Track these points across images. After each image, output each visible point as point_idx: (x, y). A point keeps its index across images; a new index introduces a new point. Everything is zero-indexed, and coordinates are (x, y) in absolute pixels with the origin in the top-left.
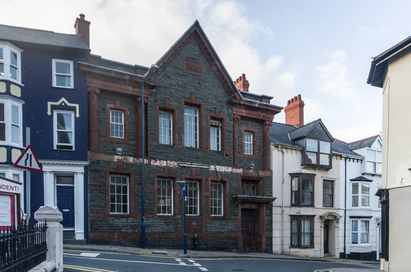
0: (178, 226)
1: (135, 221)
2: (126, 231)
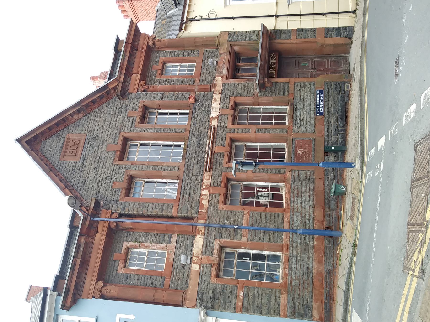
0: (303, 176)
1: (294, 245)
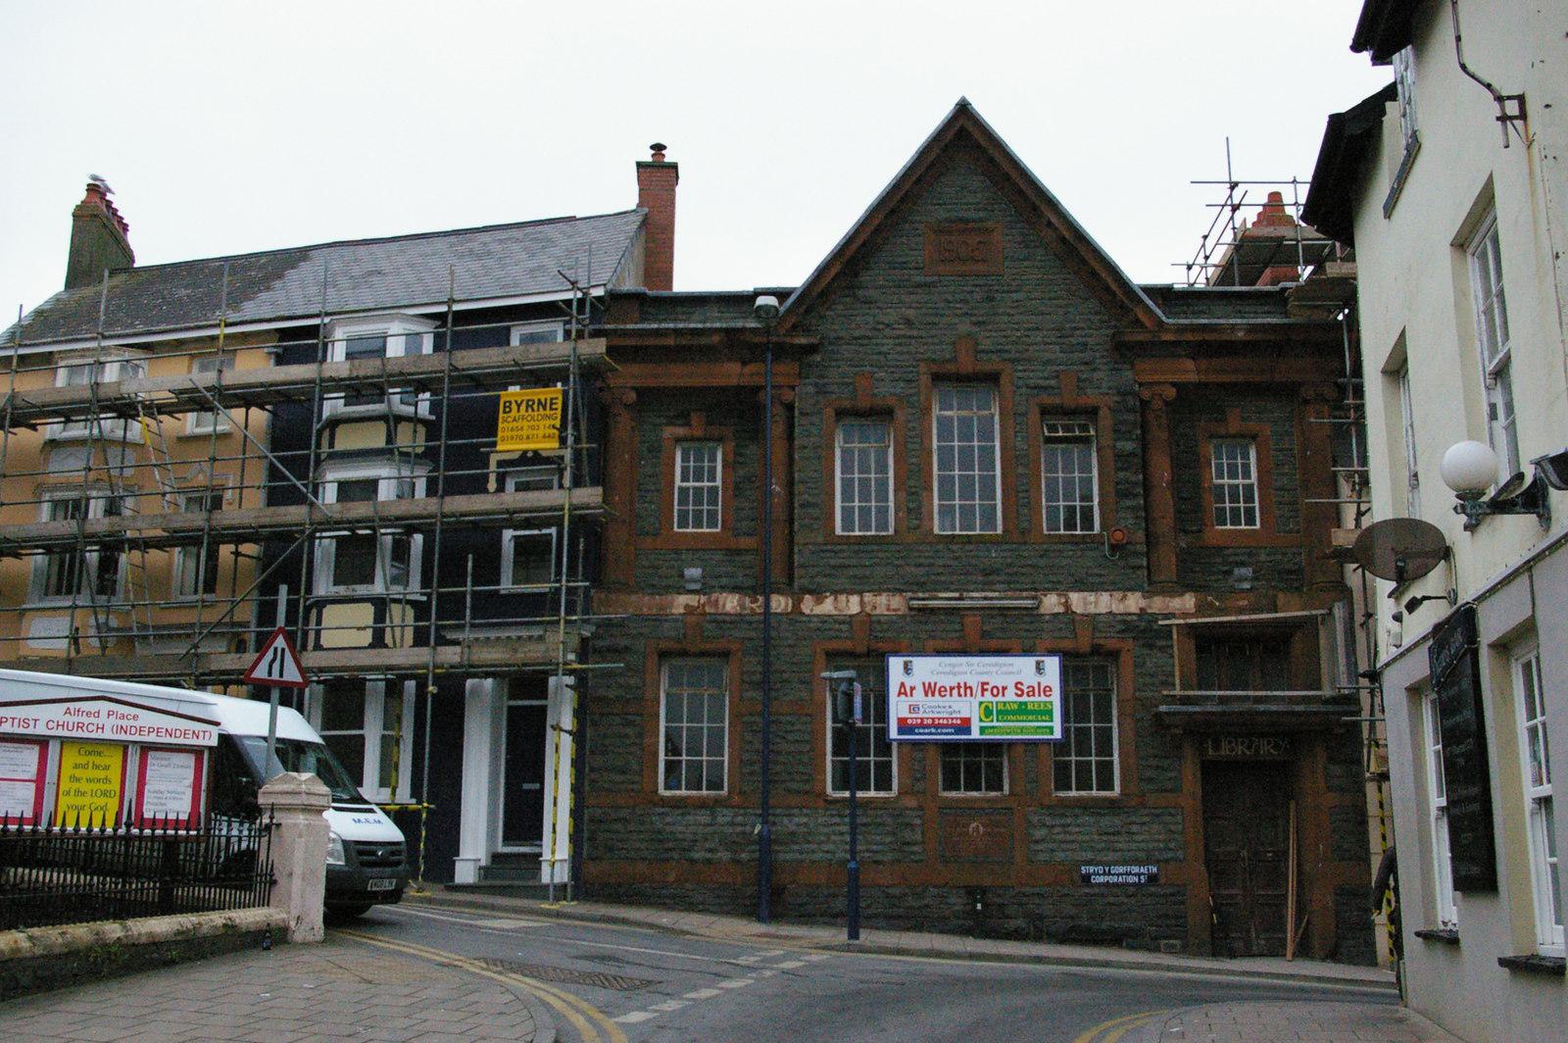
0: (907, 835)
1: (740, 819)
2: (709, 855)
